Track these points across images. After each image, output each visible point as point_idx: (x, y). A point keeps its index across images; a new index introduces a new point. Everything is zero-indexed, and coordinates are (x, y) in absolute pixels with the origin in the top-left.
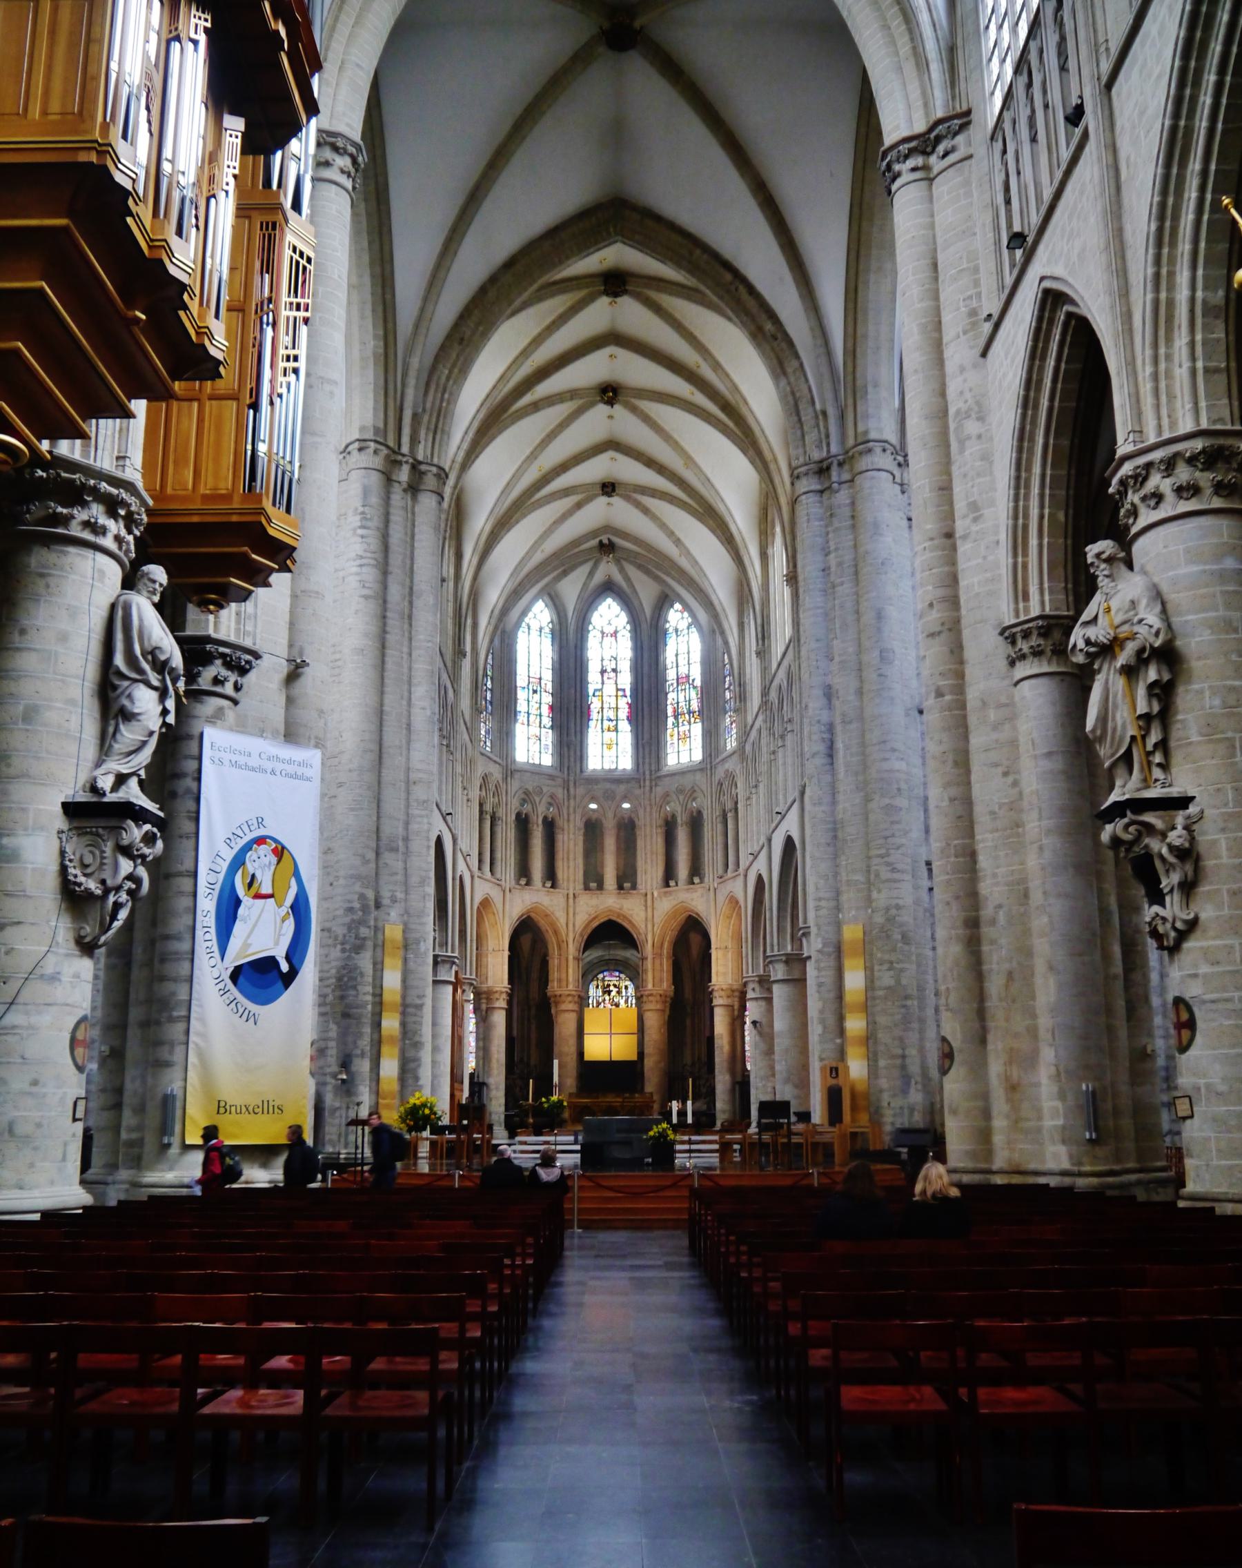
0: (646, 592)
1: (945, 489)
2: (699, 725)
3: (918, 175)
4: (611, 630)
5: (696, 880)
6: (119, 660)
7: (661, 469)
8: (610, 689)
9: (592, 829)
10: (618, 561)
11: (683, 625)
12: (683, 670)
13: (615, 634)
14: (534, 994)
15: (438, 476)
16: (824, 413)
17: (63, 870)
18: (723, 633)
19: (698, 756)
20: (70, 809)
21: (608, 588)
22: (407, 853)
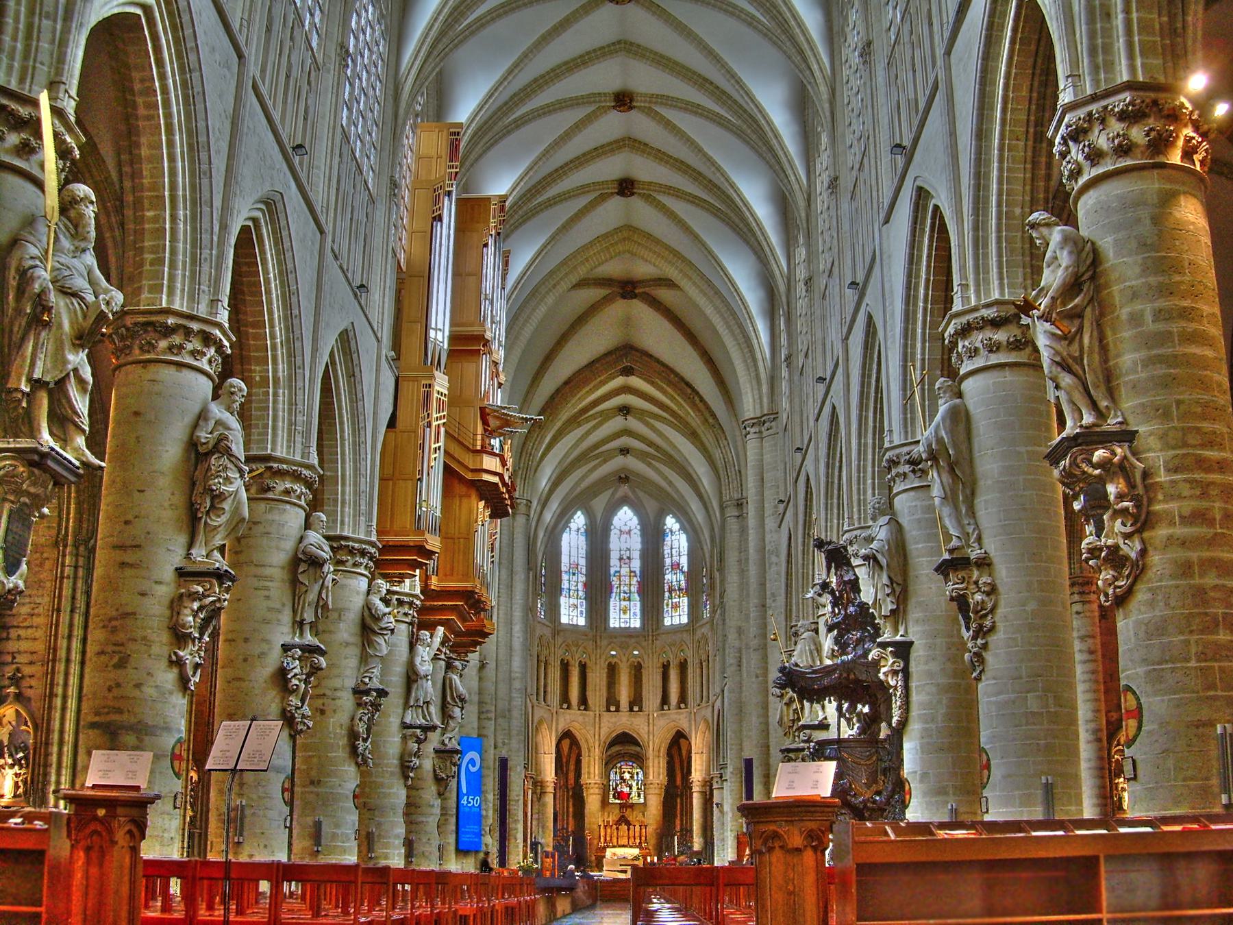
0: (651, 506)
1: (763, 584)
2: (686, 599)
3: (756, 436)
4: (627, 529)
5: (683, 706)
6: (449, 699)
7: (658, 448)
8: (625, 571)
9: (612, 670)
10: (630, 487)
11: (676, 527)
12: (675, 559)
13: (629, 532)
14: (571, 781)
15: (527, 505)
16: (740, 472)
17: (435, 771)
18: (700, 542)
19: (685, 620)
20: (437, 751)
21: (624, 501)
22: (510, 719)
